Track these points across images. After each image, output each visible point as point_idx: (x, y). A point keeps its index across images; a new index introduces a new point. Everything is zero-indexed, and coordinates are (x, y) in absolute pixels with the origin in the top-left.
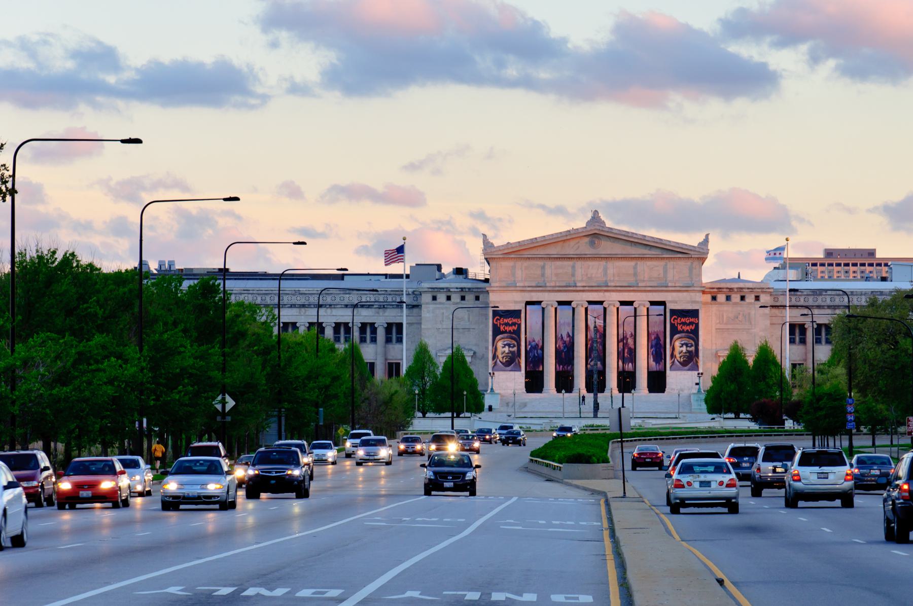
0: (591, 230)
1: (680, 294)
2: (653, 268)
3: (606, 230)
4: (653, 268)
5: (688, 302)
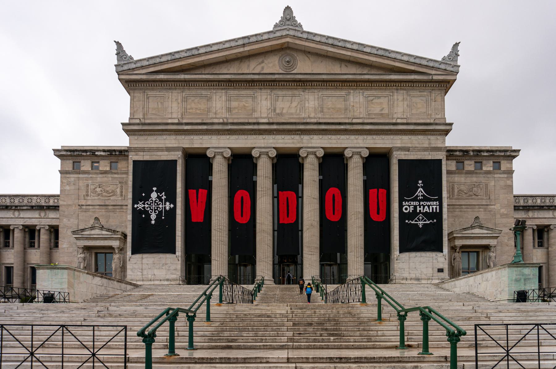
0: (282, 37)
1: (413, 138)
2: (372, 100)
3: (305, 36)
4: (372, 100)
5: (425, 149)
